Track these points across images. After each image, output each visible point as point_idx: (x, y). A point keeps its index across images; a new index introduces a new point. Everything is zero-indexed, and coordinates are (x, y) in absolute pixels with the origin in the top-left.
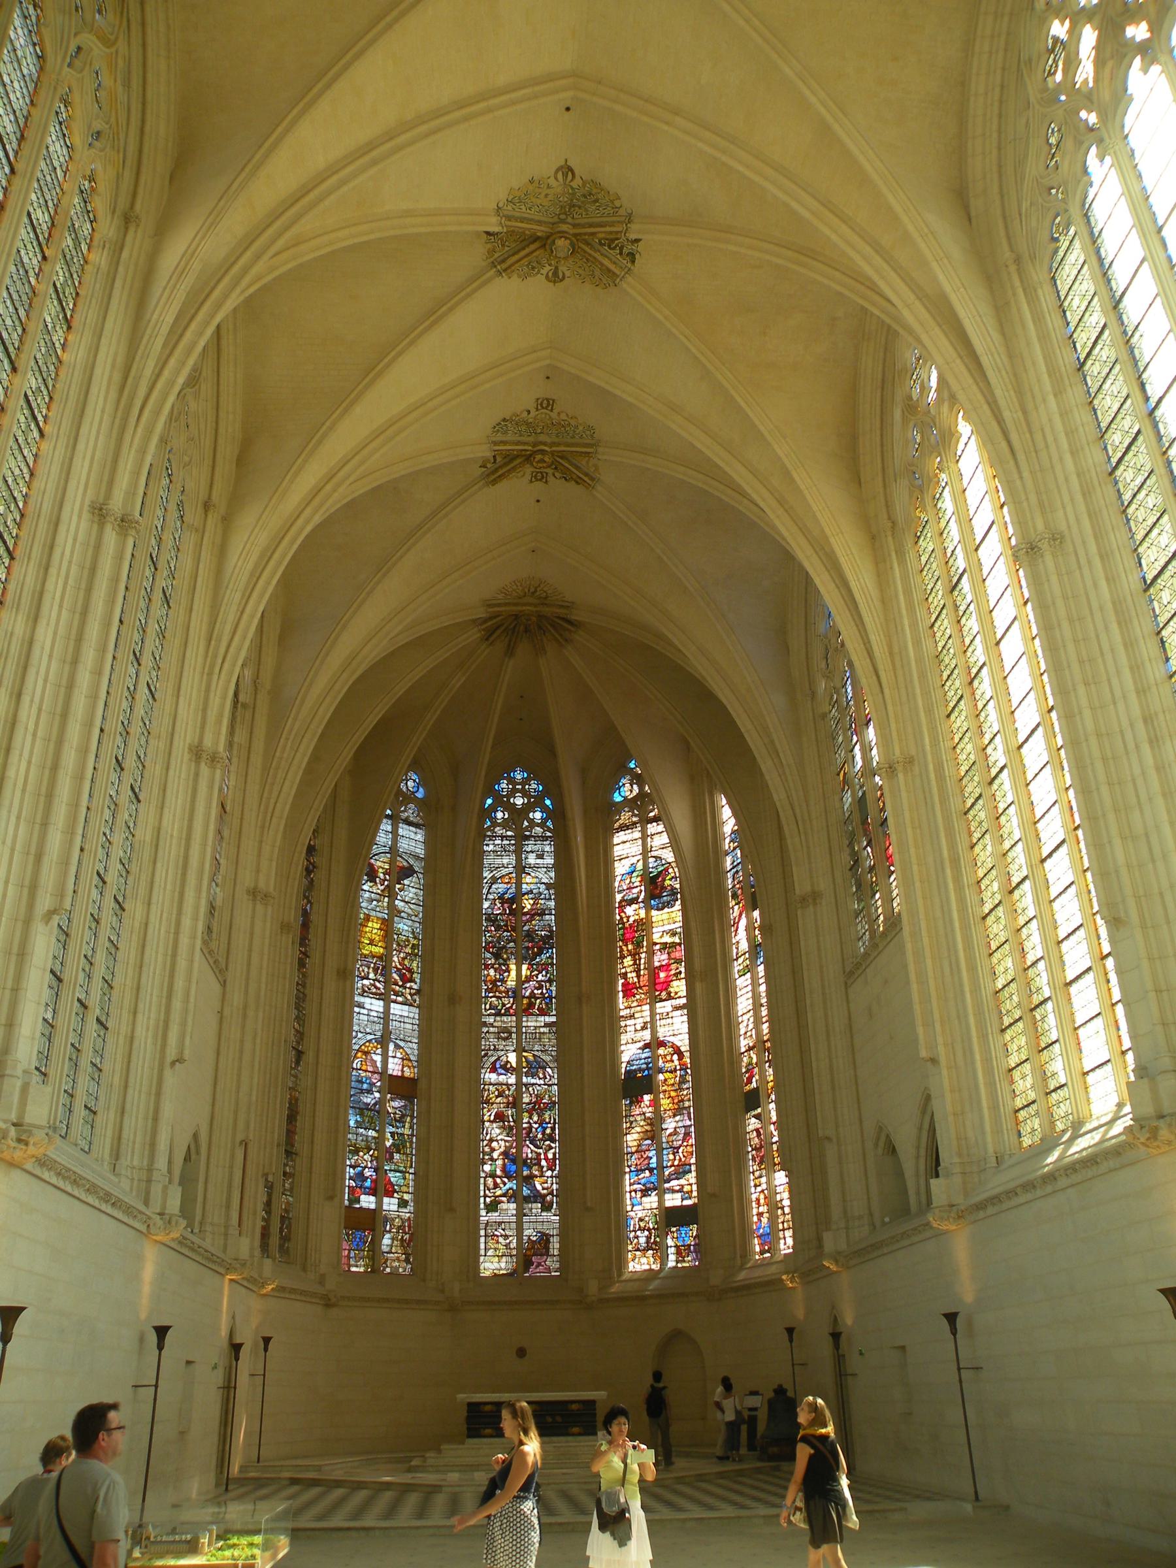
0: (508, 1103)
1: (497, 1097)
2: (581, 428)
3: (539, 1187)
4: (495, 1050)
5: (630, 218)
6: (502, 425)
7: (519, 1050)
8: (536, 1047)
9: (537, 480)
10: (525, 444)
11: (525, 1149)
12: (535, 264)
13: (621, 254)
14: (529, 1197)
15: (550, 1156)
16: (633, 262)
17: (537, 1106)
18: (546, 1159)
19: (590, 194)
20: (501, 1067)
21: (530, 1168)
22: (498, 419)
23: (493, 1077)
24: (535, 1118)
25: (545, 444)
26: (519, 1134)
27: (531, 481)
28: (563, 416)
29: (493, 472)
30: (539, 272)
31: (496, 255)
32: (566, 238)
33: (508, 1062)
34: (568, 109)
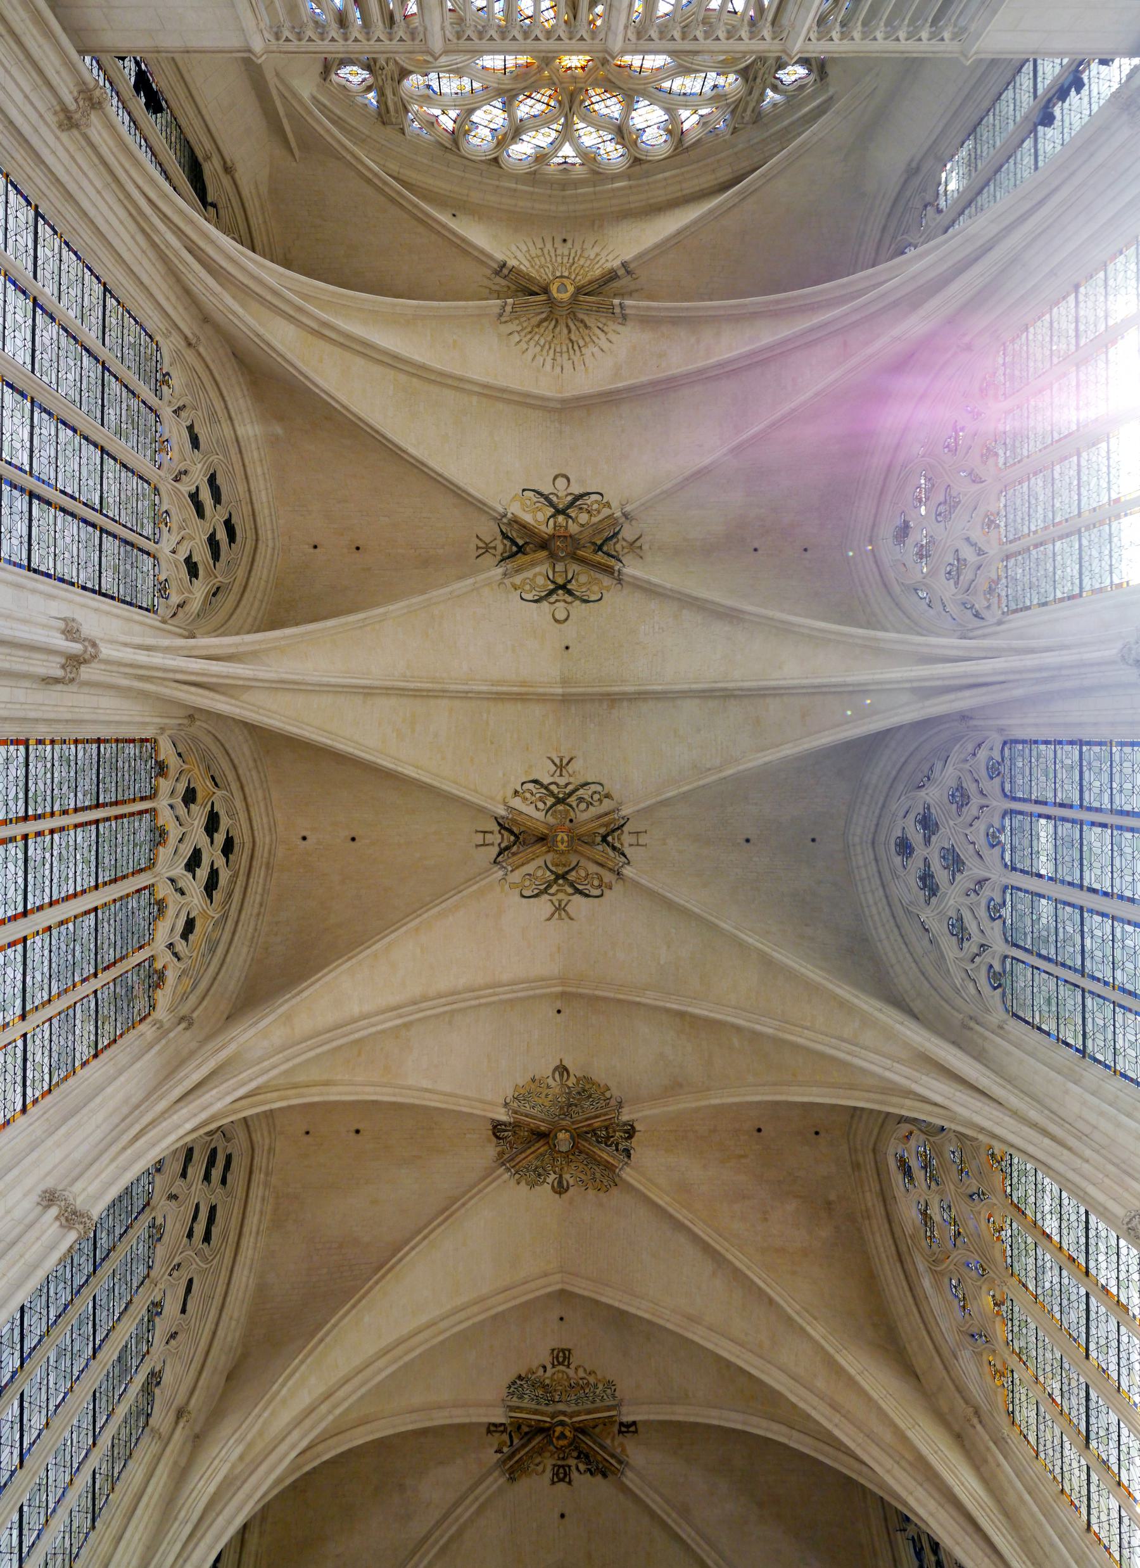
2: (600, 1386)
5: (620, 1105)
6: (518, 1384)
9: (561, 1480)
10: (542, 1414)
12: (541, 1170)
13: (617, 1150)
16: (629, 1157)
19: (584, 1090)
22: (512, 1376)
25: (564, 1413)
27: (553, 1483)
28: (581, 1373)
29: (511, 1457)
30: (544, 1182)
31: (506, 1157)
32: (567, 1131)
34: (559, 1012)
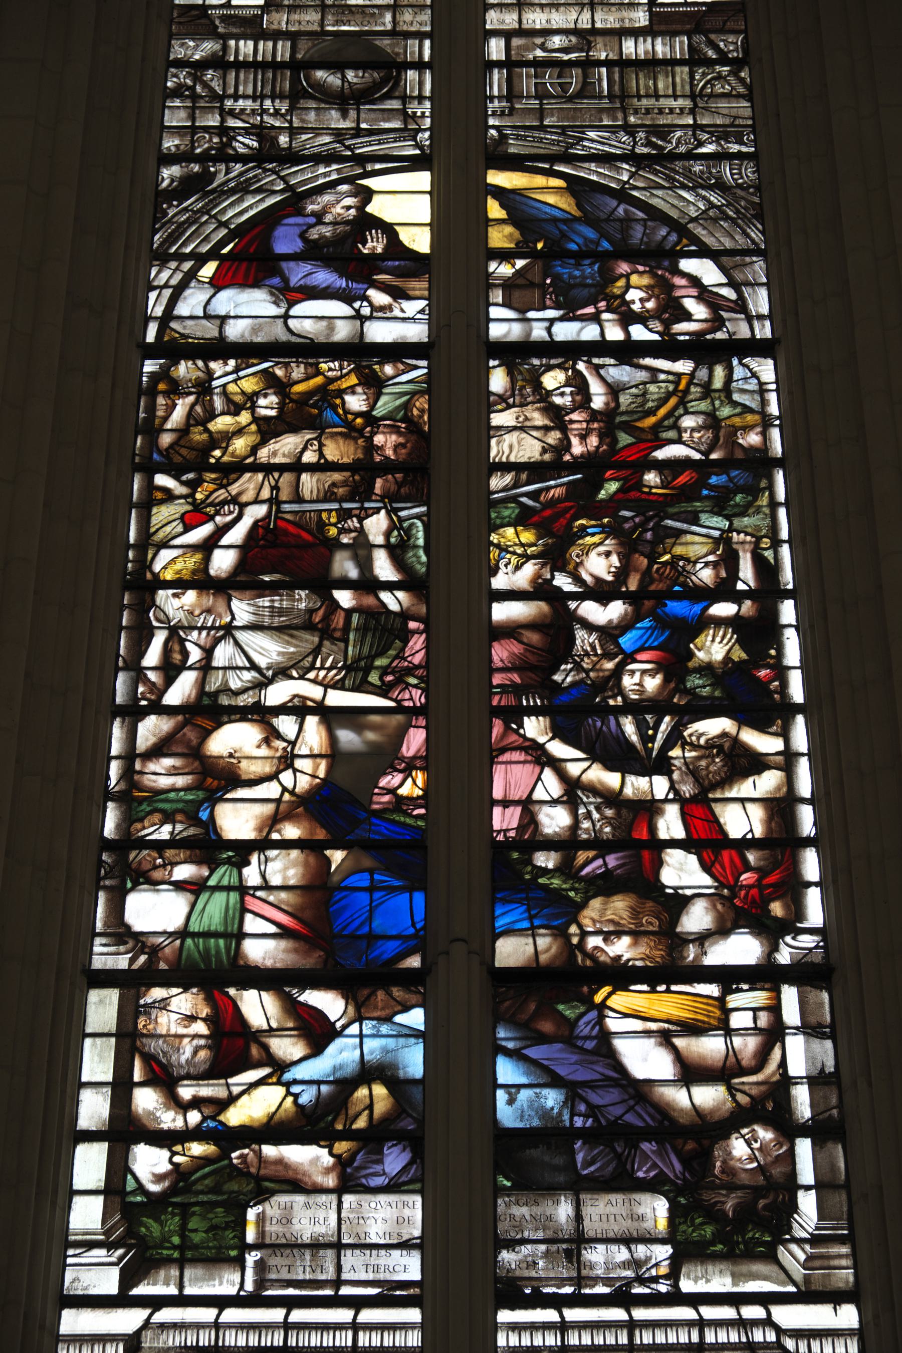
0: (365, 470)
1: (268, 430)
3: (646, 1060)
4: (269, 154)
7: (458, 164)
8: (594, 140)
11: (509, 778)
14: (548, 1135)
15: (740, 820)
17: (608, 484)
18: (707, 841)
20: (314, 252)
21: (555, 910)
23: (248, 310)
24: (599, 564)
26: (465, 681)
33: (366, 223)
